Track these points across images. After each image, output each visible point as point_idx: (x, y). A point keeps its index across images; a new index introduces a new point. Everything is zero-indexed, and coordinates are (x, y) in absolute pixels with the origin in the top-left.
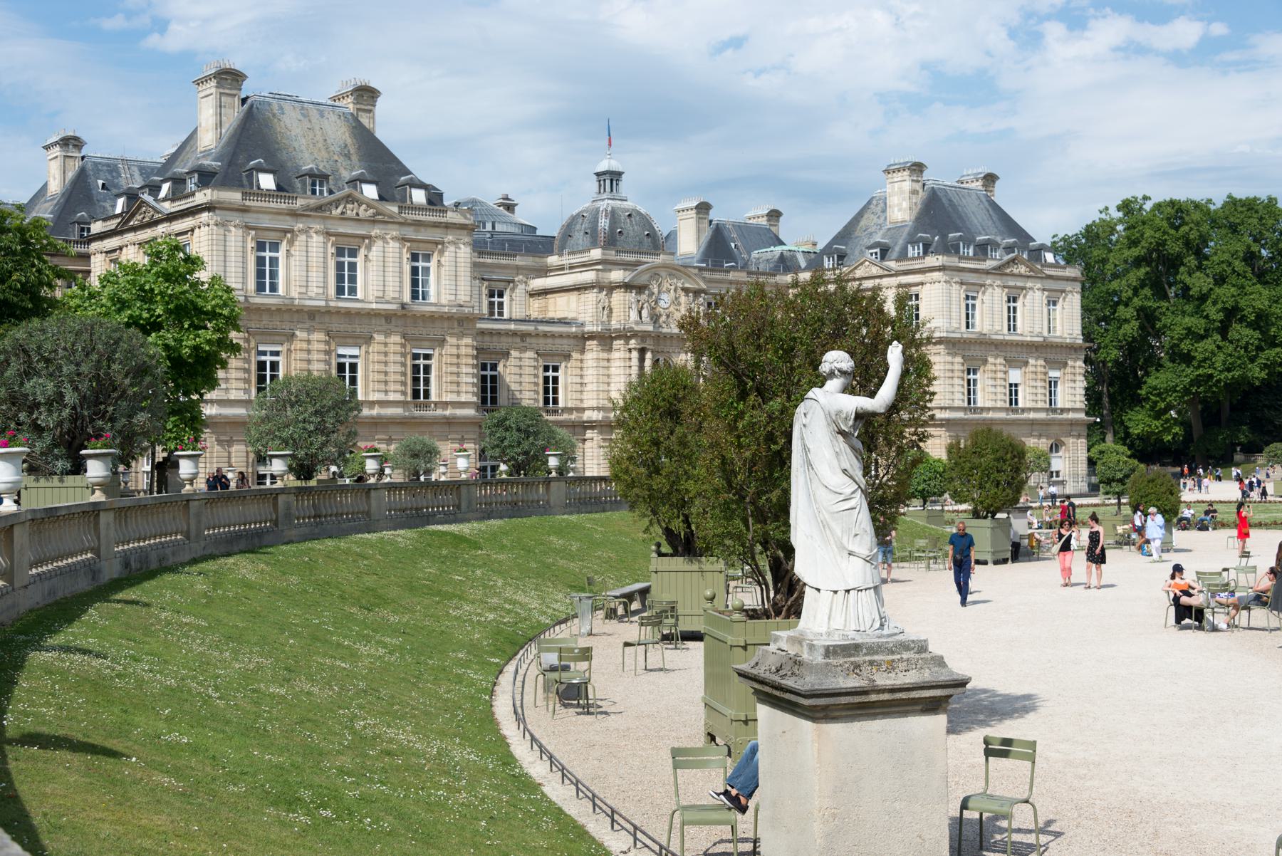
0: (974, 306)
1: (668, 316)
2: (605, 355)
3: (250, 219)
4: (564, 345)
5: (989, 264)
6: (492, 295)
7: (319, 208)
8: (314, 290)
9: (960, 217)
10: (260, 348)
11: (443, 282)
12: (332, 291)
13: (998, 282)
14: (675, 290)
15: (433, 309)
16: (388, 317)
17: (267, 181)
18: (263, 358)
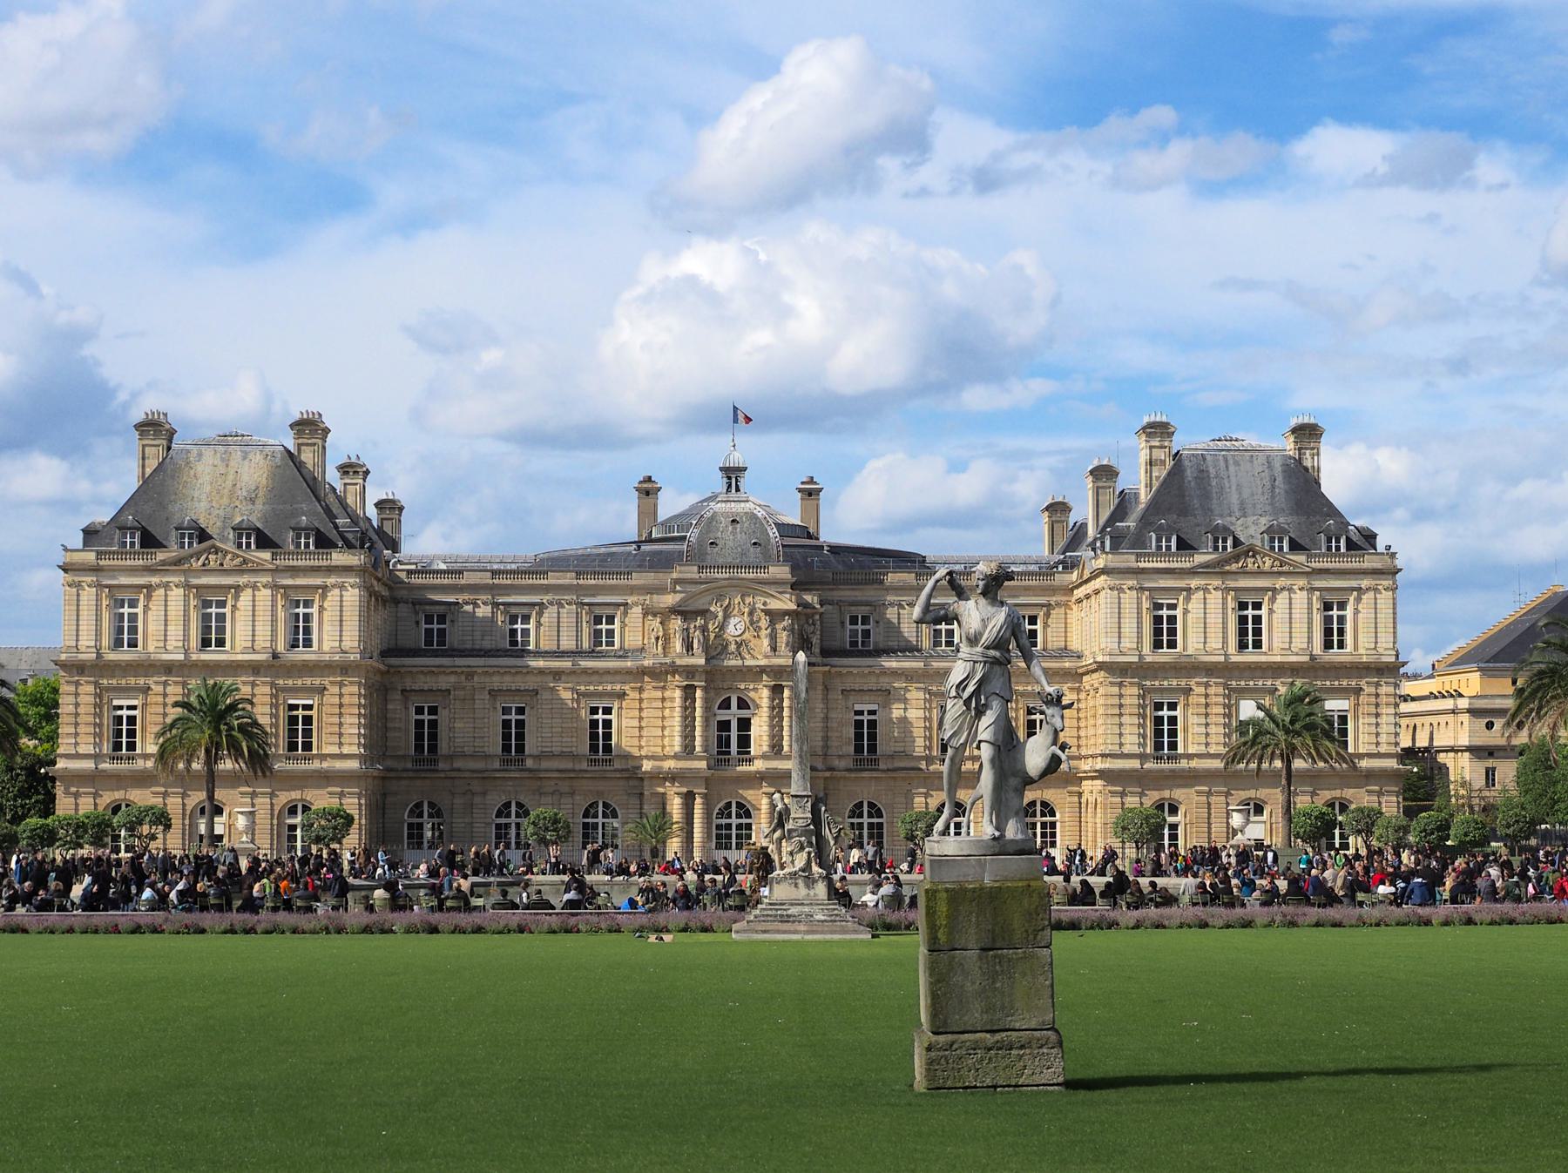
0: (1172, 620)
1: (739, 645)
2: (659, 694)
5: (1199, 559)
6: (598, 620)
7: (178, 562)
8: (171, 644)
9: (1206, 495)
10: (116, 703)
11: (326, 627)
12: (194, 642)
13: (1217, 582)
14: (751, 614)
15: (313, 657)
16: (255, 668)
18: (119, 713)
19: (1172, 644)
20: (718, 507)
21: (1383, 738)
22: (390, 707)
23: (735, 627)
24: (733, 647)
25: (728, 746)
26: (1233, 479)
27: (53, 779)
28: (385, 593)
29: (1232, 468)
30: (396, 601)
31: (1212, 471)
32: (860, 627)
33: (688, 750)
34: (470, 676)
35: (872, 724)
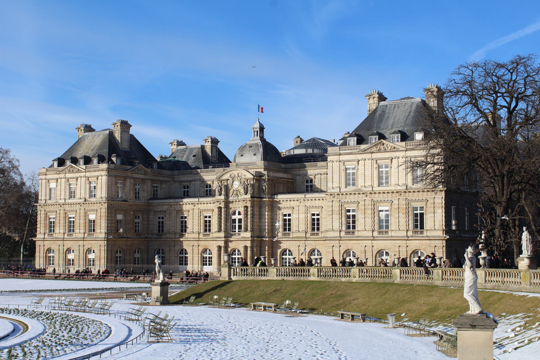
3: (48, 177)
4: (211, 206)
12: (67, 197)
17: (56, 164)
19: (354, 184)
20: (248, 143)
21: (437, 223)
22: (151, 217)
23: (236, 185)
24: (235, 193)
25: (235, 229)
26: (394, 114)
27: (35, 241)
28: (168, 179)
29: (395, 110)
30: (175, 182)
31: (387, 111)
32: (309, 184)
33: (220, 230)
34: (171, 206)
35: (289, 220)
